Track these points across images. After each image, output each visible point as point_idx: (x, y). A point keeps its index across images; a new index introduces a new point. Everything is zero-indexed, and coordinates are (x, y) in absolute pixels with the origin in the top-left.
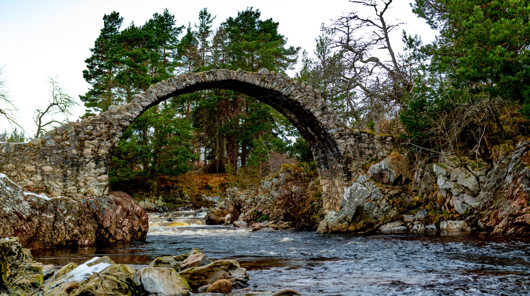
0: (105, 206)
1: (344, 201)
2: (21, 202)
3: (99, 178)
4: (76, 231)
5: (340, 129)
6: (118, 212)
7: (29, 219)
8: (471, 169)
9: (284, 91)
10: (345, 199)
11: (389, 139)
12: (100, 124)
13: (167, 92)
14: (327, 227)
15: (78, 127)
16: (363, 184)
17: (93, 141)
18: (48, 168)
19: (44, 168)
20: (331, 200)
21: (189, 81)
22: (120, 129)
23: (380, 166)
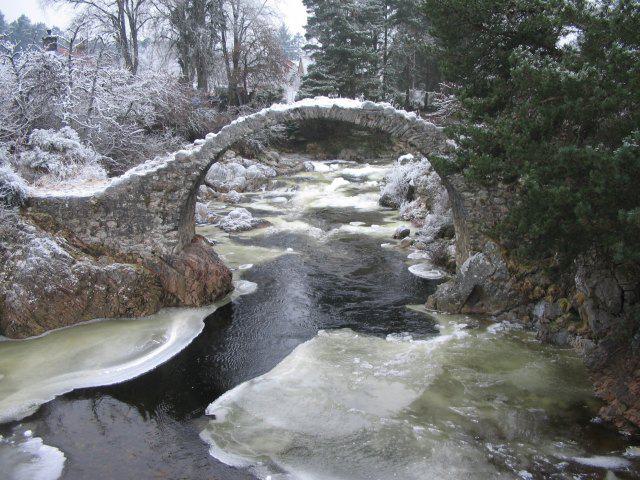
2: (67, 276)
4: (130, 305)
6: (187, 274)
7: (78, 293)
15: (143, 177)
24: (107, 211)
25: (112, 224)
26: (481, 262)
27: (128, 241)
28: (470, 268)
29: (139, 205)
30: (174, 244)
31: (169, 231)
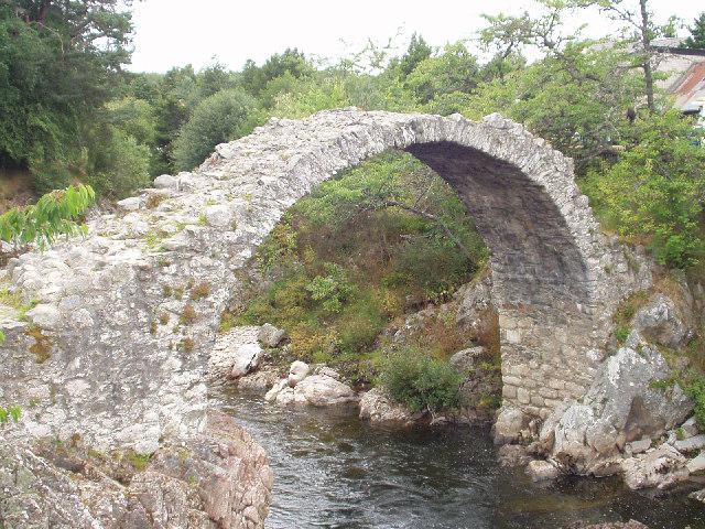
0: (218, 470)
3: (190, 393)
9: (524, 165)
10: (613, 383)
13: (330, 172)
14: (585, 442)
15: (142, 269)
18: (78, 388)
19: (70, 387)
20: (533, 363)
22: (233, 267)
23: (661, 314)
24: (69, 357)
25: (78, 388)
27: (109, 423)
28: (621, 373)
29: (136, 335)
30: (201, 413)
31: (194, 384)
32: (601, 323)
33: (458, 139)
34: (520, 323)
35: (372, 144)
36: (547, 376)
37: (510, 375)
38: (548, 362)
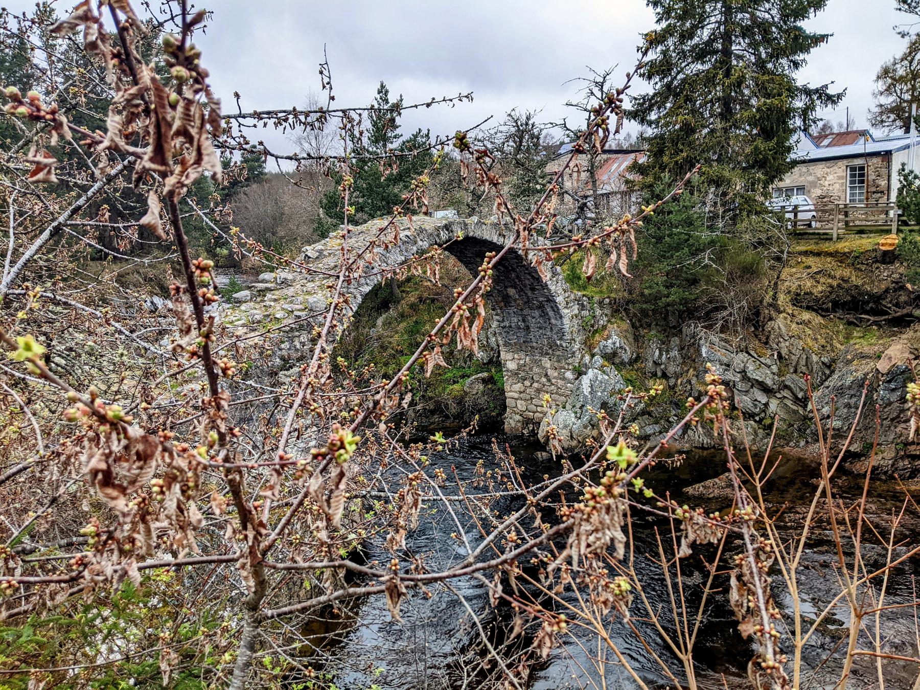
1: (585, 397)
5: (567, 295)
8: (755, 355)
11: (607, 300)
12: (299, 336)
14: (572, 437)
16: (601, 368)
17: (291, 371)
20: (527, 383)
21: (420, 243)
23: (614, 343)
26: (600, 378)
28: (591, 386)
32: (574, 353)
33: (476, 235)
34: (516, 356)
35: (420, 243)
36: (538, 391)
37: (511, 391)
38: (537, 382)
